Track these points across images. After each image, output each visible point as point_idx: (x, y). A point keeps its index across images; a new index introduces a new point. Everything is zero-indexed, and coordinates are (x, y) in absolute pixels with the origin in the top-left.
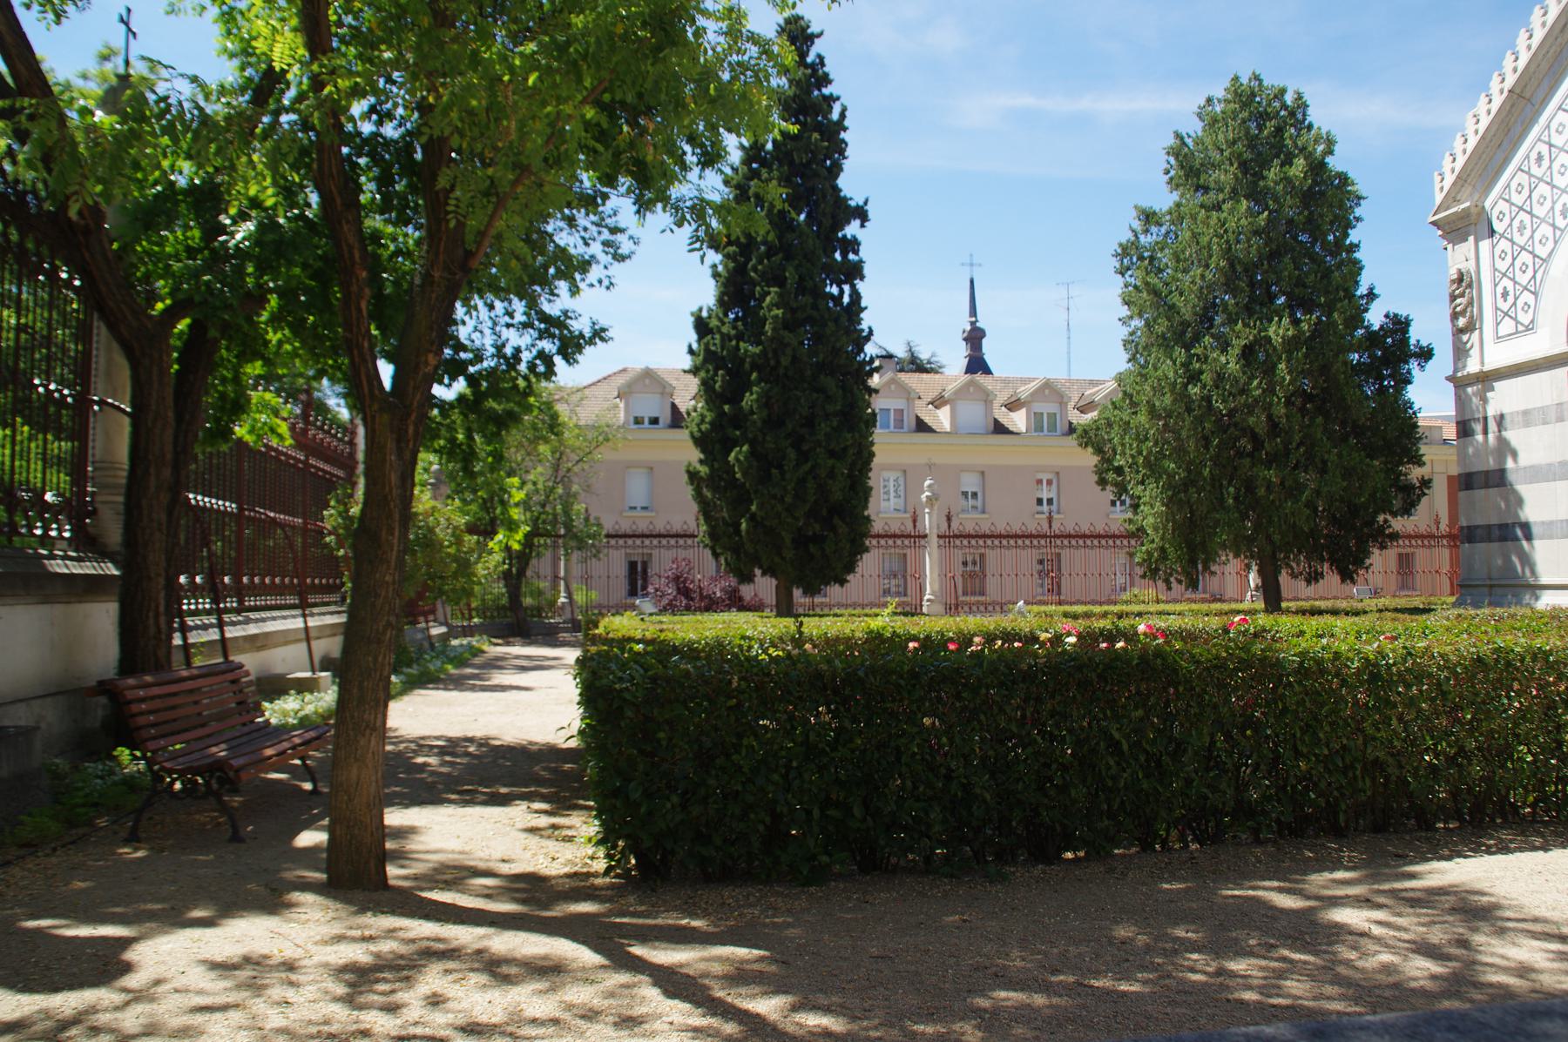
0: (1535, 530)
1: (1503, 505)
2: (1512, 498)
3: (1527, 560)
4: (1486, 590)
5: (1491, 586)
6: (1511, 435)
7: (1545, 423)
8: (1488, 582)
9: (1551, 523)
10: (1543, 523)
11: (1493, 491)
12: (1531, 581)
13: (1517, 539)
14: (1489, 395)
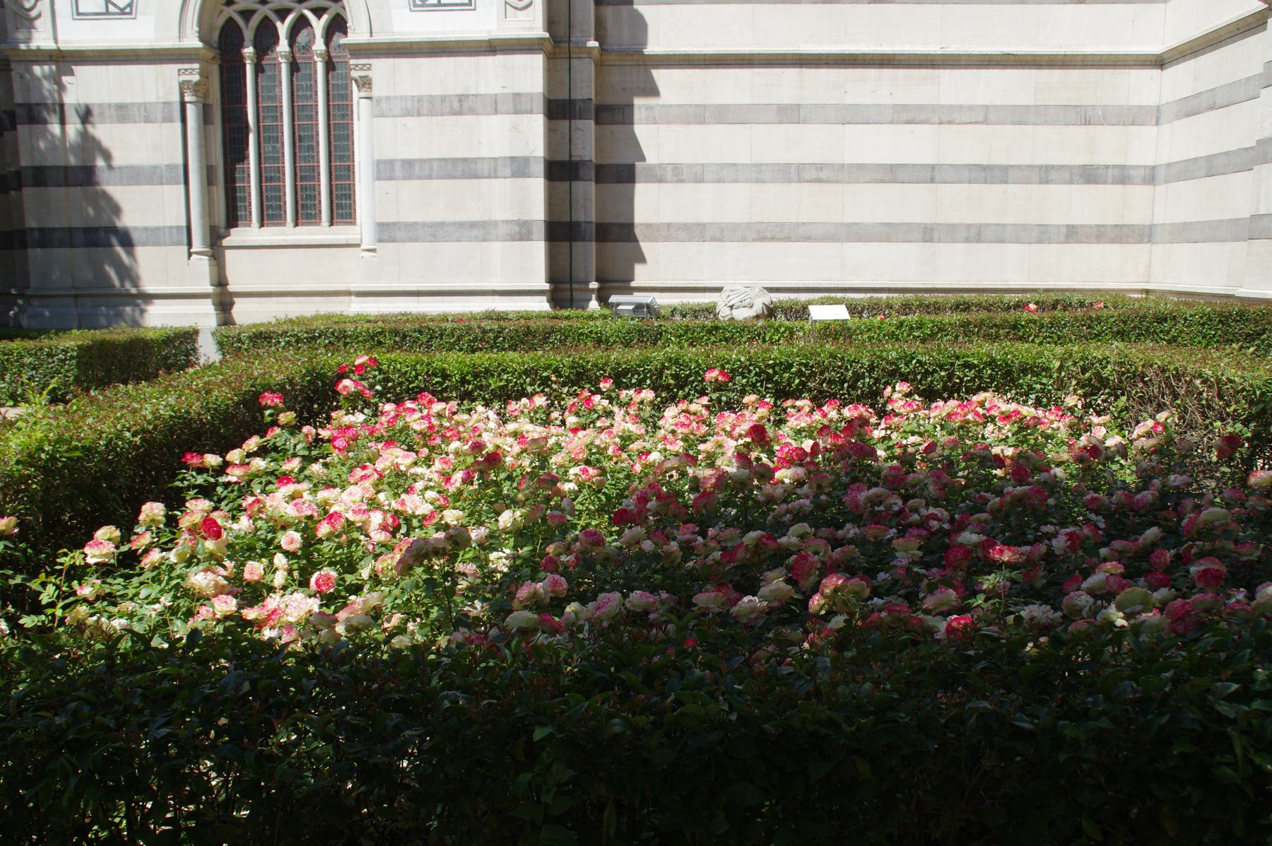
0: (135, 237)
1: (91, 211)
2: (103, 203)
3: (128, 274)
4: (71, 300)
5: (77, 296)
6: (102, 132)
8: (74, 292)
9: (157, 229)
10: (146, 229)
11: (76, 192)
12: (134, 291)
13: (111, 245)
14: (66, 79)
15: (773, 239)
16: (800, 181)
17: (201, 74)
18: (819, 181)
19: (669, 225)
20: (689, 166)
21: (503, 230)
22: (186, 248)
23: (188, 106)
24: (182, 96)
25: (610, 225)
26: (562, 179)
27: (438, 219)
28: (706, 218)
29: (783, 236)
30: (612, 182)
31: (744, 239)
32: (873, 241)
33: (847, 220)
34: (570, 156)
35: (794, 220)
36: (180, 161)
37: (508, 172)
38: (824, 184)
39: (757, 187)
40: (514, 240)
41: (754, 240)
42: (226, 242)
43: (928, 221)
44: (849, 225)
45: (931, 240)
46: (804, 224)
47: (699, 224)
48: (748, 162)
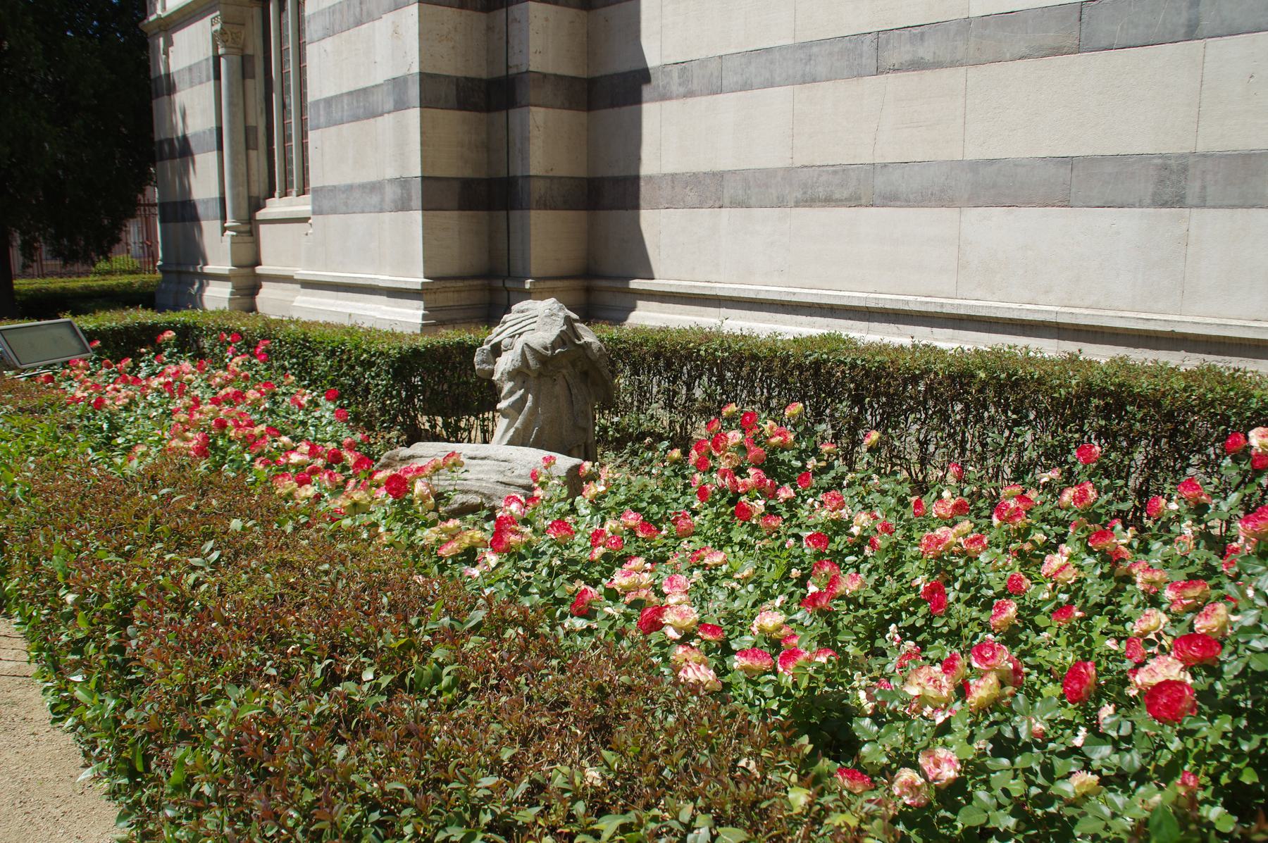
7: (201, 83)
15: (829, 201)
16: (878, 72)
17: (224, 22)
18: (917, 65)
19: (674, 176)
20: (703, 62)
21: (391, 193)
22: (218, 223)
23: (222, 60)
24: (215, 48)
25: (602, 179)
26: (498, 109)
27: (348, 180)
28: (725, 163)
29: (846, 194)
30: (605, 108)
31: (780, 203)
32: (1029, 203)
33: (974, 153)
34: (508, 67)
35: (868, 160)
36: (213, 124)
37: (390, 105)
38: (928, 74)
39: (803, 92)
40: (397, 210)
41: (797, 205)
42: (260, 215)
43: (1172, 146)
44: (974, 166)
45: (1178, 201)
46: (885, 165)
47: (714, 174)
48: (790, 42)
